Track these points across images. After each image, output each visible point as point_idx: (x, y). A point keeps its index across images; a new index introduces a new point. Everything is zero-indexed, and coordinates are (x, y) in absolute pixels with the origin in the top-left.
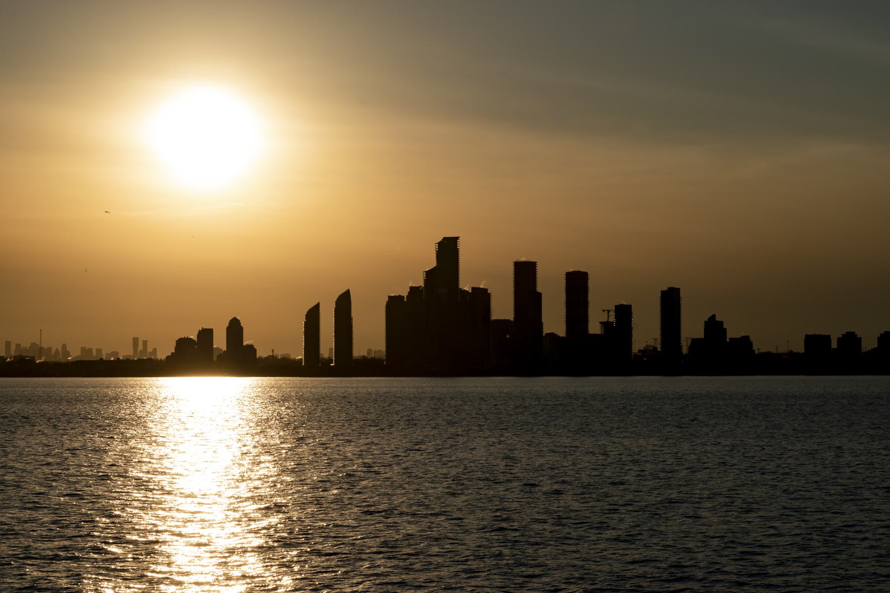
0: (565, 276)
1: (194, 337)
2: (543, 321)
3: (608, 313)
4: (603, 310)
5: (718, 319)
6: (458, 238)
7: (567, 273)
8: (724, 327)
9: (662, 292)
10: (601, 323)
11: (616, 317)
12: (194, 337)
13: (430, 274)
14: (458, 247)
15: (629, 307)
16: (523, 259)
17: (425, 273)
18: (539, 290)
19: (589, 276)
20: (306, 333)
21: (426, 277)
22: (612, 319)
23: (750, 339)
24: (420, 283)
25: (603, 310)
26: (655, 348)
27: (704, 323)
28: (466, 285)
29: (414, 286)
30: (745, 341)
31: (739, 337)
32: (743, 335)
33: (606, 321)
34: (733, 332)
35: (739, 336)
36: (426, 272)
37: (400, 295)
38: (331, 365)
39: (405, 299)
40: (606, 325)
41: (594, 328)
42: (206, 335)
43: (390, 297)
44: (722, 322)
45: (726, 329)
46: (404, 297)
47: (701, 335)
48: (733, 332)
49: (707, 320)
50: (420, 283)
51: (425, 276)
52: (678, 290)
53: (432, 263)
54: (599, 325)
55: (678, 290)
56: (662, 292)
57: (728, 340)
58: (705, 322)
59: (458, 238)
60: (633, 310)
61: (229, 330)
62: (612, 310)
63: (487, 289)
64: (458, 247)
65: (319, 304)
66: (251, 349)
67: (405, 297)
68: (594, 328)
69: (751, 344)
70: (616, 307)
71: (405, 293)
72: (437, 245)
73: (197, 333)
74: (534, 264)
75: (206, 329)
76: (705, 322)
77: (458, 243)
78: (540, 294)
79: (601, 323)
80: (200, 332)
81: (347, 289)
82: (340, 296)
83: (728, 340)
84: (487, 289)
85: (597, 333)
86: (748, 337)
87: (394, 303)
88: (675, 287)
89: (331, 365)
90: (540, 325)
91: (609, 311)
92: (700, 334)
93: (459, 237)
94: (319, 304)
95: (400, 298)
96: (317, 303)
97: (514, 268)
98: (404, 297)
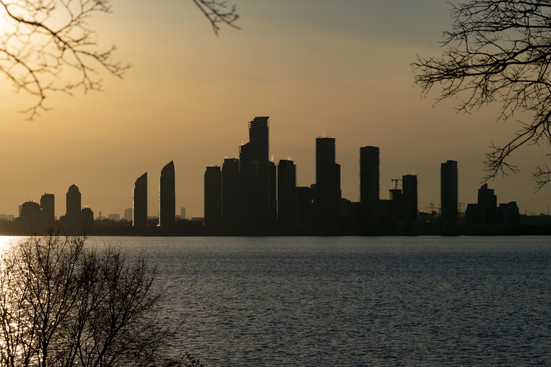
0: (360, 151)
1: (39, 202)
2: (342, 188)
3: (396, 182)
4: (392, 180)
5: (489, 187)
6: (268, 118)
7: (361, 148)
8: (495, 194)
9: (442, 164)
10: (390, 190)
11: (403, 186)
12: (39, 202)
13: (244, 148)
14: (268, 126)
15: (415, 177)
16: (324, 136)
17: (240, 148)
18: (338, 161)
19: (379, 151)
20: (135, 198)
21: (241, 151)
22: (400, 187)
23: (516, 205)
24: (236, 155)
25: (392, 180)
26: (434, 213)
27: (478, 191)
28: (274, 158)
29: (228, 158)
30: (513, 206)
31: (507, 203)
32: (510, 201)
33: (394, 189)
34: (502, 199)
35: (507, 202)
36: (241, 147)
37: (216, 166)
38: (158, 225)
39: (221, 169)
40: (394, 192)
41: (384, 195)
42: (48, 200)
43: (208, 168)
44: (493, 190)
45: (496, 196)
46: (220, 167)
47: (475, 201)
48: (502, 199)
49: (480, 188)
50: (236, 155)
51: (240, 150)
52: (456, 163)
53: (245, 139)
54: (389, 192)
55: (456, 162)
56: (442, 164)
57: (498, 205)
58: (479, 190)
59: (268, 118)
60: (418, 179)
61: (68, 195)
62: (400, 180)
63: (292, 162)
64: (268, 126)
65: (146, 173)
66: (89, 212)
67: (221, 168)
68: (384, 195)
69: (517, 209)
70: (403, 176)
71: (220, 164)
72: (250, 123)
73: (40, 198)
74: (333, 140)
75: (48, 194)
76: (479, 190)
77: (268, 122)
78: (339, 166)
79: (390, 190)
80: (43, 197)
81: (171, 161)
82: (165, 167)
83: (498, 205)
84: (292, 162)
85: (387, 199)
86: (516, 202)
87: (211, 173)
88: (453, 160)
89: (158, 225)
90: (339, 192)
91: (397, 181)
92: (475, 201)
93: (269, 117)
94: (146, 173)
95: (217, 168)
96: (144, 173)
97: (316, 143)
98: (220, 167)
